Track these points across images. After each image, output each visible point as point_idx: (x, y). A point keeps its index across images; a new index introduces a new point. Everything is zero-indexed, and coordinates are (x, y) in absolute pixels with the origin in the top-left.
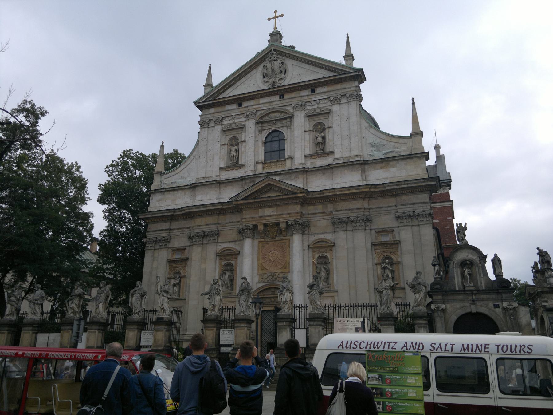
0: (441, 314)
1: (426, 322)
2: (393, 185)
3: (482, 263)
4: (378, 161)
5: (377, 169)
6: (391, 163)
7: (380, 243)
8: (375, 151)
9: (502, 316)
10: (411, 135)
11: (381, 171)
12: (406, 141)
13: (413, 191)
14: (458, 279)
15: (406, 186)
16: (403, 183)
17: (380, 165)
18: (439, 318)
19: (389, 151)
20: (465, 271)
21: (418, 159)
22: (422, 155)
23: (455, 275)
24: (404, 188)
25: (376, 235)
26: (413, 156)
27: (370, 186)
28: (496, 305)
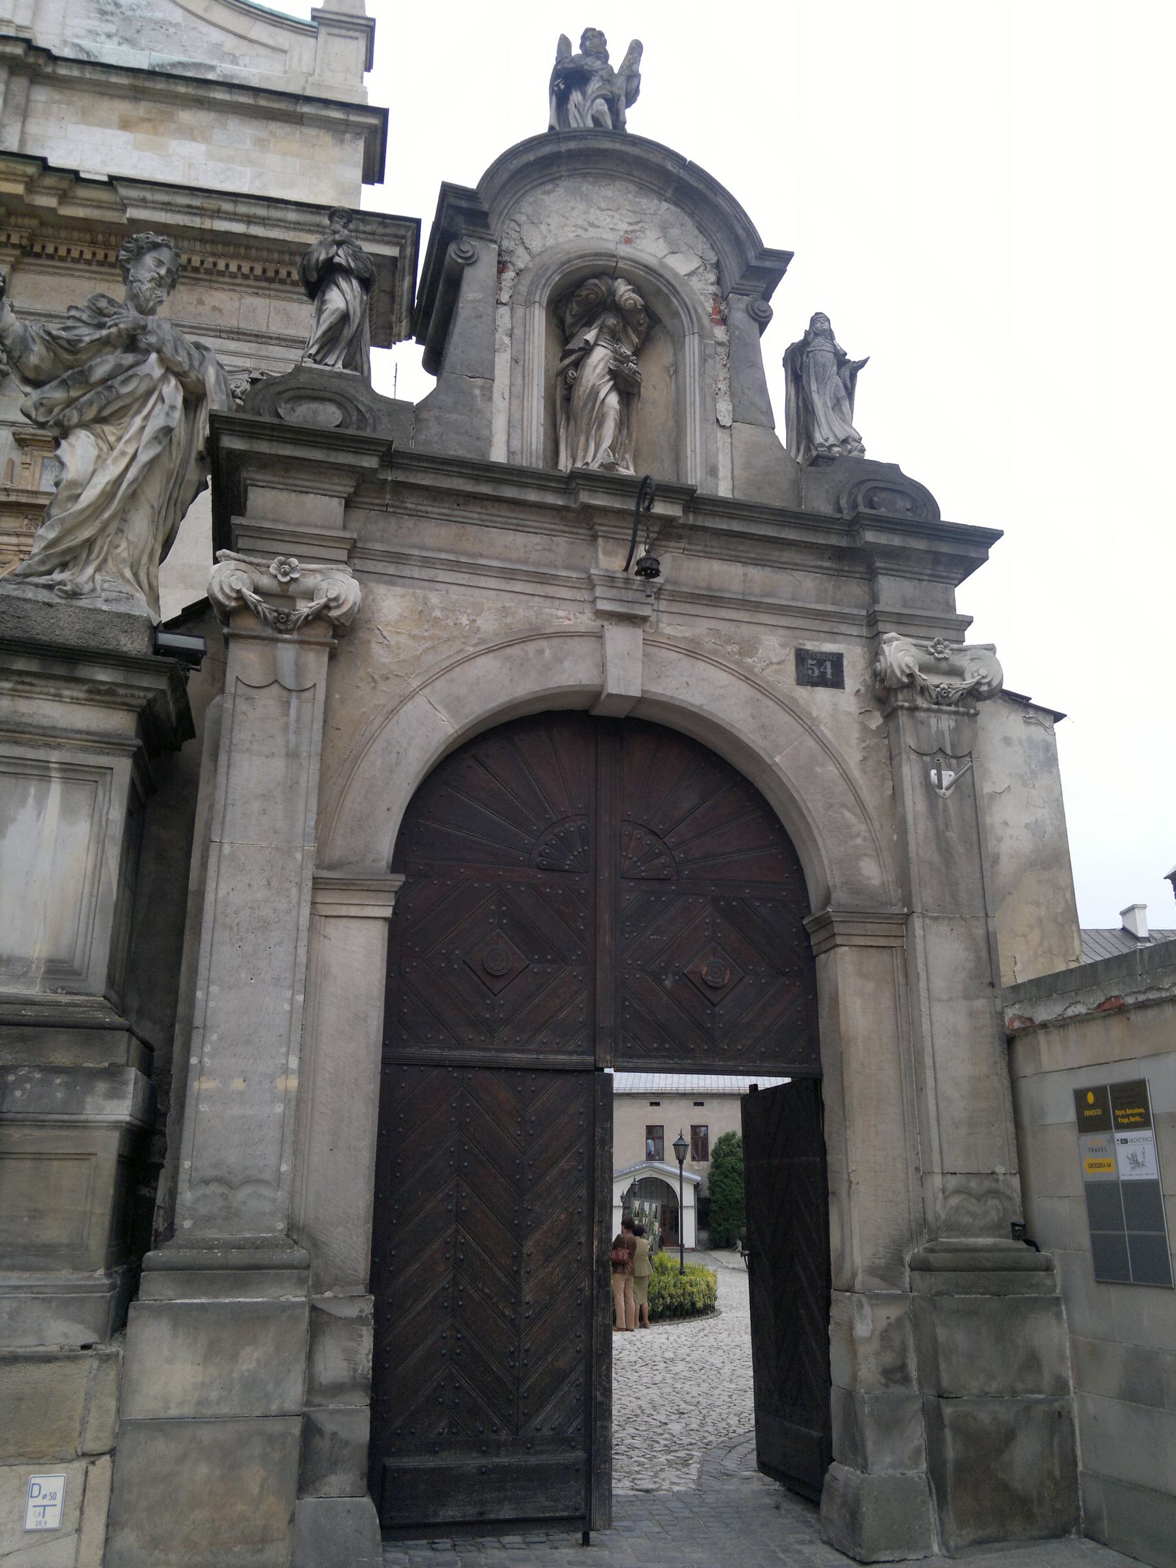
0: (299, 670)
1: (120, 722)
2: (167, 207)
3: (739, 316)
4: (114, 79)
5: (103, 124)
6: (186, 116)
7: (23, 499)
8: (109, 36)
9: (853, 756)
10: (314, 18)
11: (119, 139)
12: (283, 38)
13: (270, 273)
14: (517, 396)
15: (238, 228)
16: (227, 206)
17: (123, 107)
18: (268, 701)
19: (184, 59)
20: (588, 349)
21: (326, 138)
22: (353, 118)
23: (502, 362)
24: (227, 238)
25: (18, 457)
26: (306, 109)
27: (31, 170)
28: (821, 659)
